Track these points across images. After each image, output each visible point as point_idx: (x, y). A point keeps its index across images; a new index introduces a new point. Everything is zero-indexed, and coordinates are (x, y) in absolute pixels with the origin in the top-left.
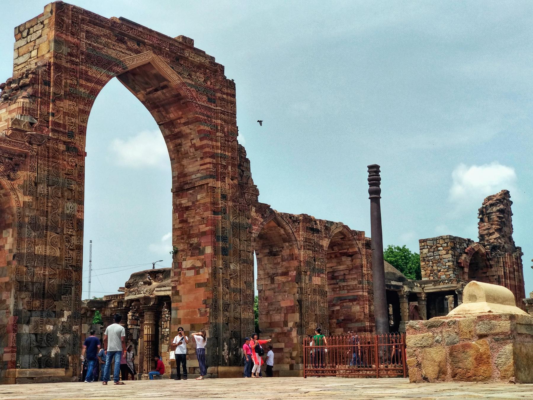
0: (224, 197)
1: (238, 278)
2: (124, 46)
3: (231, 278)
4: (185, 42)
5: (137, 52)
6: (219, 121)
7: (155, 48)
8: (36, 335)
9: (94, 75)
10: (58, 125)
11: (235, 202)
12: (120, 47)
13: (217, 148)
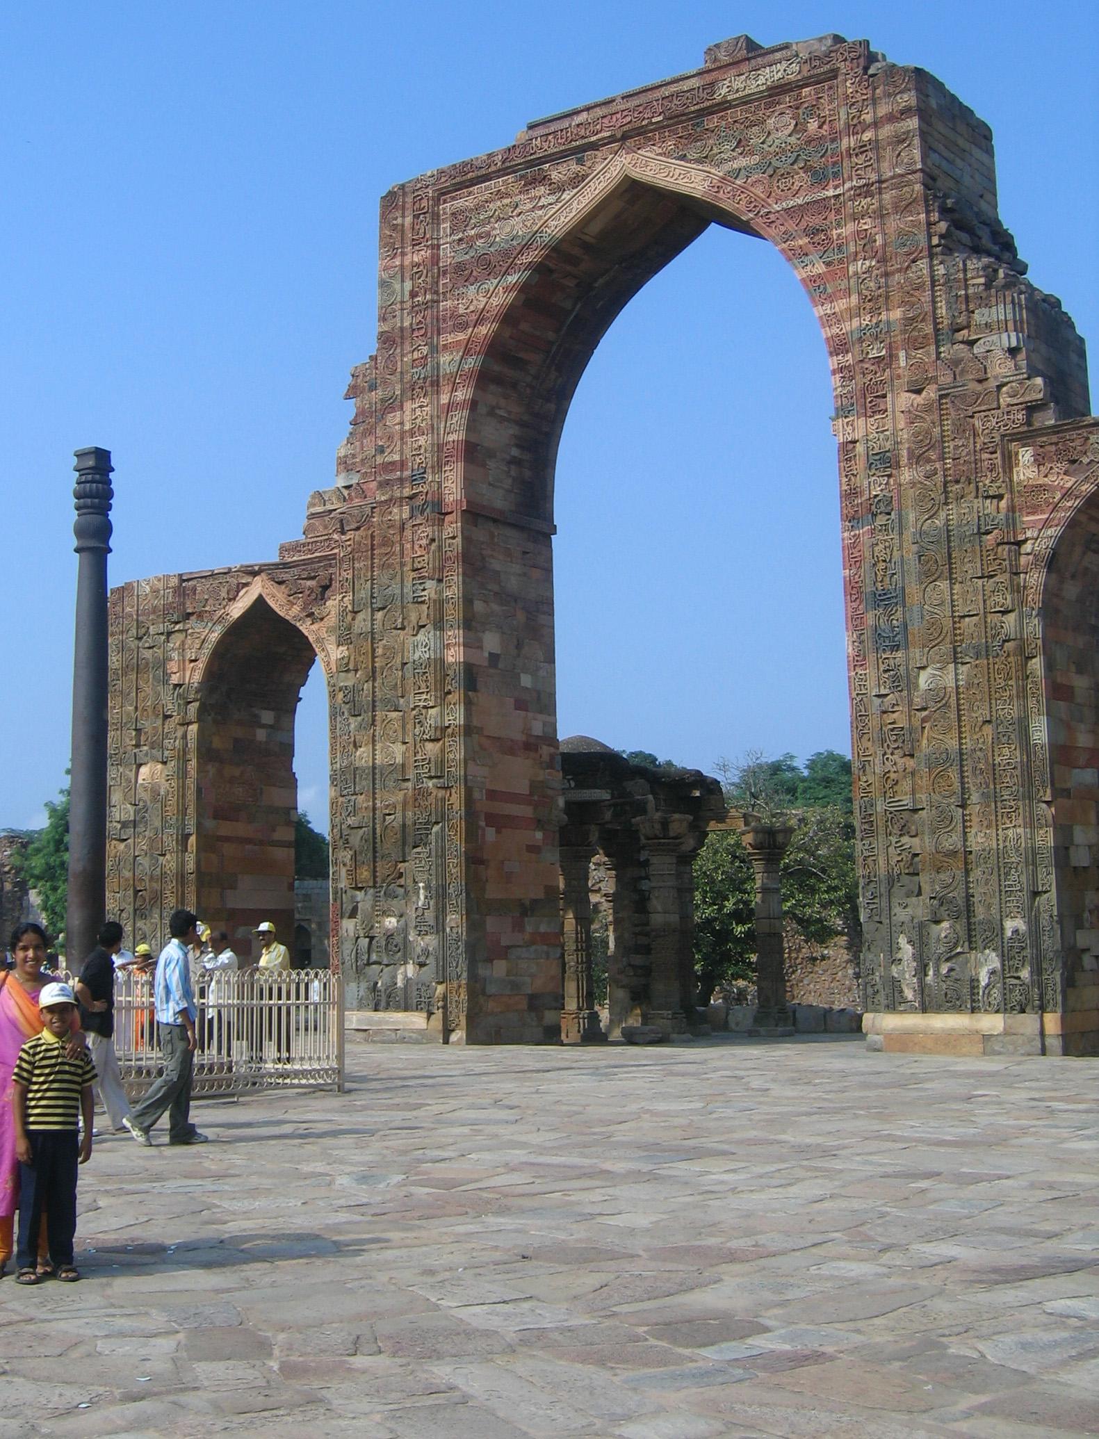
0: (885, 461)
1: (953, 715)
2: (542, 190)
3: (924, 720)
4: (715, 60)
5: (577, 181)
6: (849, 229)
7: (625, 137)
8: (372, 938)
9: (472, 308)
10: (388, 467)
11: (929, 461)
12: (531, 199)
13: (853, 313)
